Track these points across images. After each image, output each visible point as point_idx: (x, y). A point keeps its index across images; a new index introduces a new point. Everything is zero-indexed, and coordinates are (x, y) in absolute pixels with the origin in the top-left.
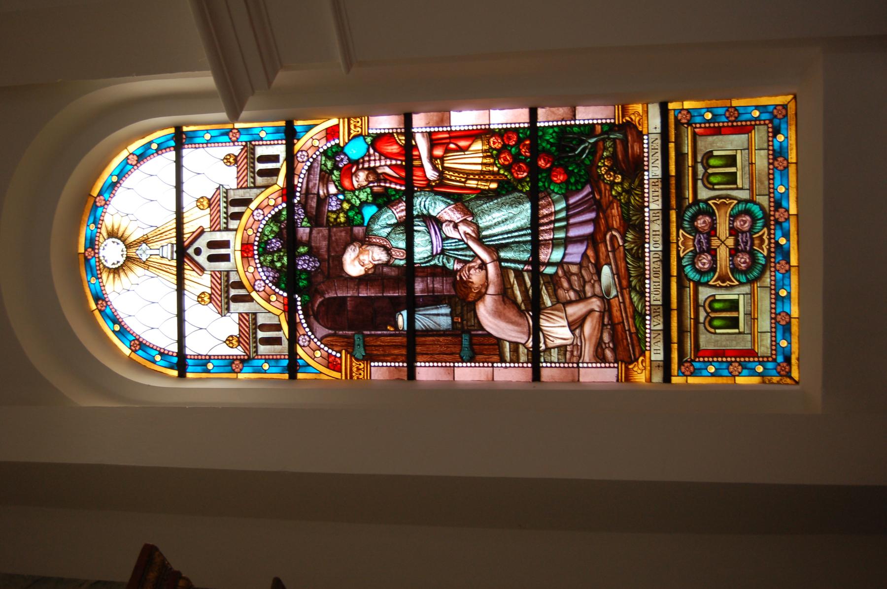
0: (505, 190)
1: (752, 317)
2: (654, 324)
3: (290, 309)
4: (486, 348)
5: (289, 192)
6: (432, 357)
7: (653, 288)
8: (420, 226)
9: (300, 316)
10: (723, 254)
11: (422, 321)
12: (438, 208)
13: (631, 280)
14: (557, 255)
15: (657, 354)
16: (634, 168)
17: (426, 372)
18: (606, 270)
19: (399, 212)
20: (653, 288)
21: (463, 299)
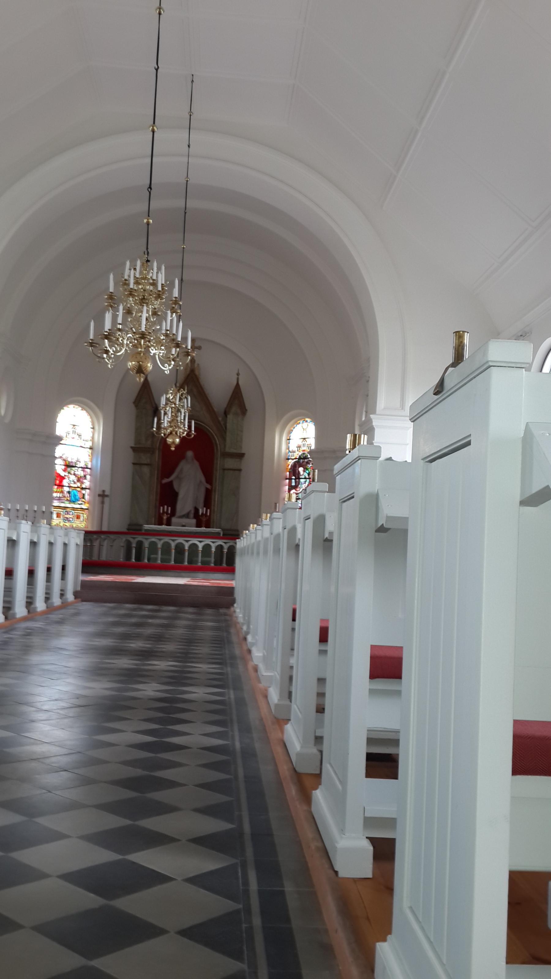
3: (296, 459)
8: (305, 480)
9: (295, 460)
11: (293, 481)
12: (307, 483)
14: (300, 502)
19: (307, 477)
21: (295, 487)
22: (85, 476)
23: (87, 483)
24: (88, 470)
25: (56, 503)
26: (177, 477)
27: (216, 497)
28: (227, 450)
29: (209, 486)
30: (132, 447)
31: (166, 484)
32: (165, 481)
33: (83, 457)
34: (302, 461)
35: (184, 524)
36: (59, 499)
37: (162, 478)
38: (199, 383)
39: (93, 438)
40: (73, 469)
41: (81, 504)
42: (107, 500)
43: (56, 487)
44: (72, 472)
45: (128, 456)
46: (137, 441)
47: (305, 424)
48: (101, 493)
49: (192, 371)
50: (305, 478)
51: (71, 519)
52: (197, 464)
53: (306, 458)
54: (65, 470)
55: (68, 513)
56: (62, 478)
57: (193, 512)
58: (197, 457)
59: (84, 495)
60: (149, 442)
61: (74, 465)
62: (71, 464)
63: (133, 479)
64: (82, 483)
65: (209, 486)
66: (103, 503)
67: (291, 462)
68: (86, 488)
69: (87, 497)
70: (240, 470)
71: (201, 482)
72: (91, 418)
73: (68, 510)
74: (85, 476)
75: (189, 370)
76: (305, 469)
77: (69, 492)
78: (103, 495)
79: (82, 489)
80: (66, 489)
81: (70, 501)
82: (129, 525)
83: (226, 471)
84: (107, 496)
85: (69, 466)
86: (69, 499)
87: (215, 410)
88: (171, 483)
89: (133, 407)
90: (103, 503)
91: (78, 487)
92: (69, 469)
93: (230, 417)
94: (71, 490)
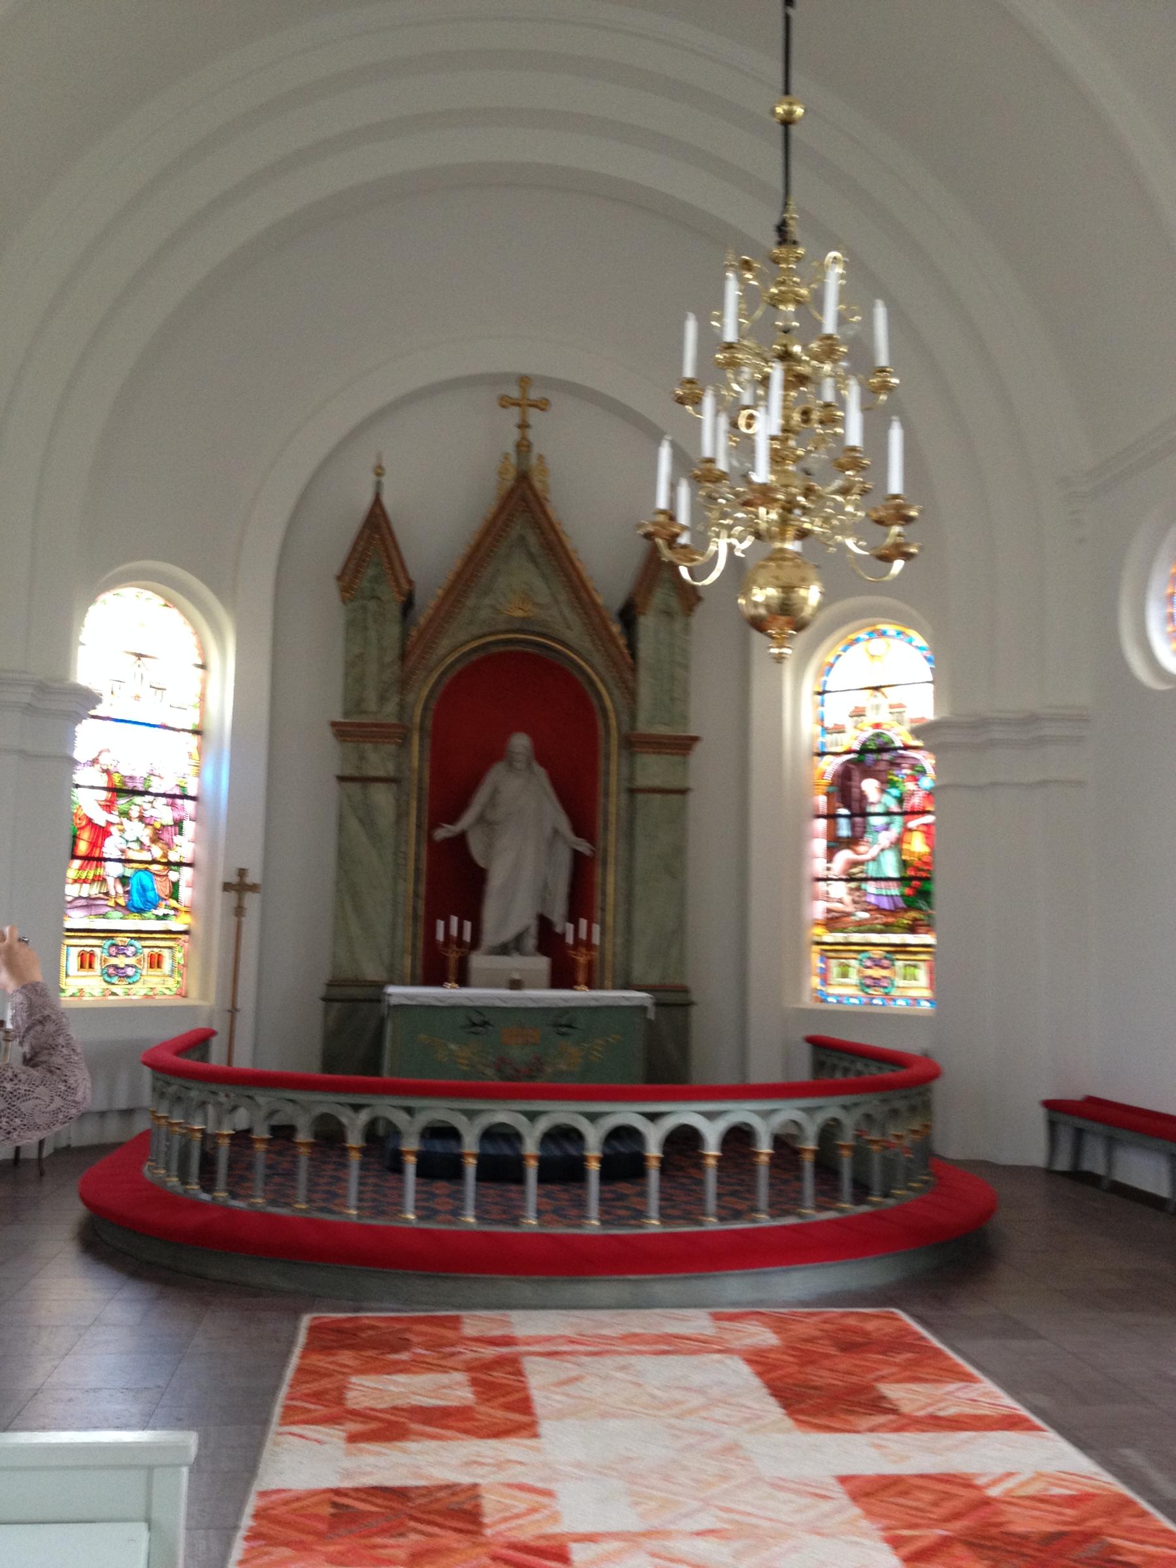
0: (904, 864)
1: (841, 985)
2: (839, 937)
4: (831, 853)
5: (906, 748)
6: (829, 827)
7: (856, 937)
10: (869, 972)
12: (895, 830)
13: (861, 927)
15: (829, 937)
16: (912, 929)
17: (821, 824)
18: (866, 915)
20: (856, 937)
21: (852, 842)
22: (178, 824)
23: (184, 847)
24: (189, 805)
25: (77, 919)
26: (481, 819)
27: (610, 881)
28: (644, 727)
29: (584, 847)
30: (334, 724)
31: (447, 841)
32: (444, 832)
33: (170, 762)
34: (876, 757)
35: (516, 976)
36: (89, 904)
37: (434, 825)
38: (545, 512)
39: (202, 698)
40: (138, 800)
41: (165, 917)
42: (252, 902)
43: (77, 863)
44: (135, 813)
45: (324, 757)
46: (354, 704)
47: (878, 644)
48: (234, 879)
49: (523, 477)
50: (888, 813)
51: (130, 971)
52: (541, 772)
53: (885, 748)
54: (108, 807)
55: (120, 950)
56: (102, 833)
57: (533, 931)
58: (542, 755)
59: (175, 885)
60: (391, 707)
61: (140, 788)
62: (130, 785)
63: (341, 827)
64: (169, 846)
65: (584, 847)
66: (239, 911)
67: (830, 766)
68: (180, 864)
69: (185, 894)
70: (683, 792)
71: (556, 832)
72: (197, 632)
73: (120, 940)
74: (178, 824)
75: (511, 476)
76: (886, 784)
77: (123, 880)
78: (238, 886)
79: (169, 864)
80: (113, 870)
81: (129, 909)
82: (331, 984)
83: (640, 797)
84: (254, 888)
85: (121, 791)
86: (122, 901)
87: (600, 600)
88: (460, 840)
89: (332, 591)
90: (239, 911)
91: (154, 862)
92: (122, 803)
93: (647, 623)
94: (128, 873)
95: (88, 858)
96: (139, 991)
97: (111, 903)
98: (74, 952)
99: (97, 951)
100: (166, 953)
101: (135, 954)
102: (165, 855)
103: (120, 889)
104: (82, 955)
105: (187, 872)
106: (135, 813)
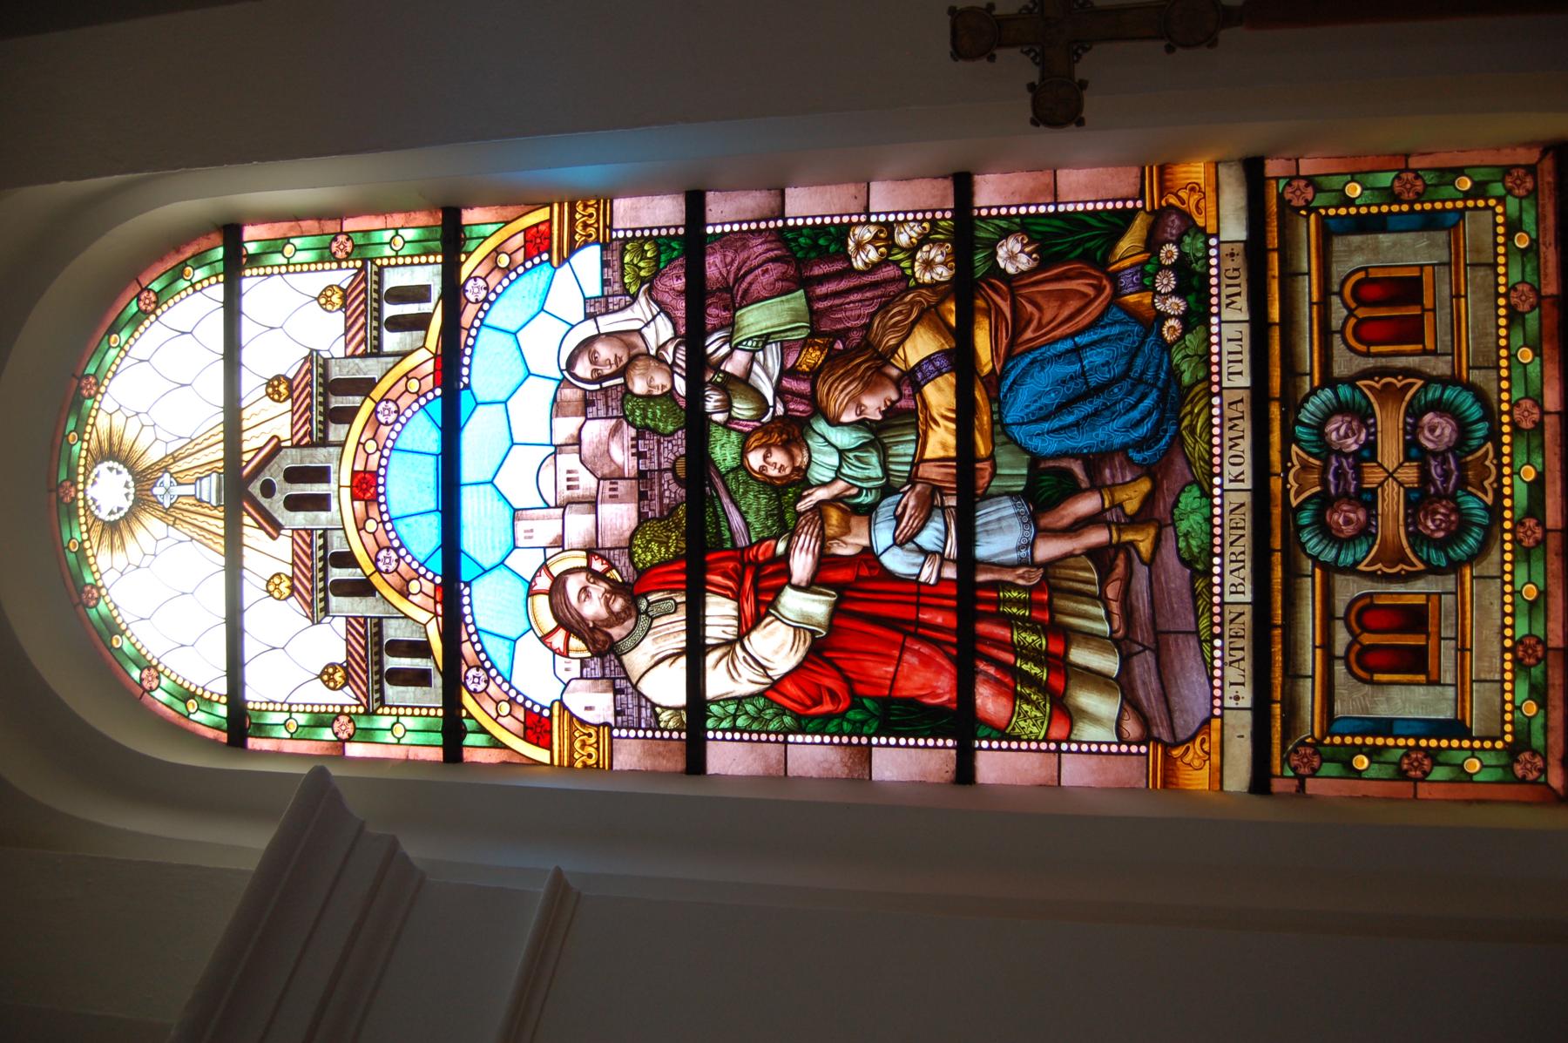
23: (891, 206)
36: (1148, 643)
40: (724, 452)
44: (771, 462)
48: (1016, 69)
51: (1438, 432)
55: (1347, 485)
61: (674, 448)
62: (673, 491)
64: (889, 286)
69: (1084, 187)
77: (1042, 495)
80: (1001, 537)
81: (1168, 458)
85: (692, 543)
86: (1132, 498)
91: (960, 359)
92: (742, 520)
94: (1013, 471)
95: (965, 659)
96: (1524, 375)
97: (1144, 541)
98: (1353, 700)
99: (1348, 590)
100: (1354, 256)
101: (1362, 415)
102: (929, 315)
103: (1087, 505)
104: (1368, 664)
105: (990, 193)
106: (771, 462)
